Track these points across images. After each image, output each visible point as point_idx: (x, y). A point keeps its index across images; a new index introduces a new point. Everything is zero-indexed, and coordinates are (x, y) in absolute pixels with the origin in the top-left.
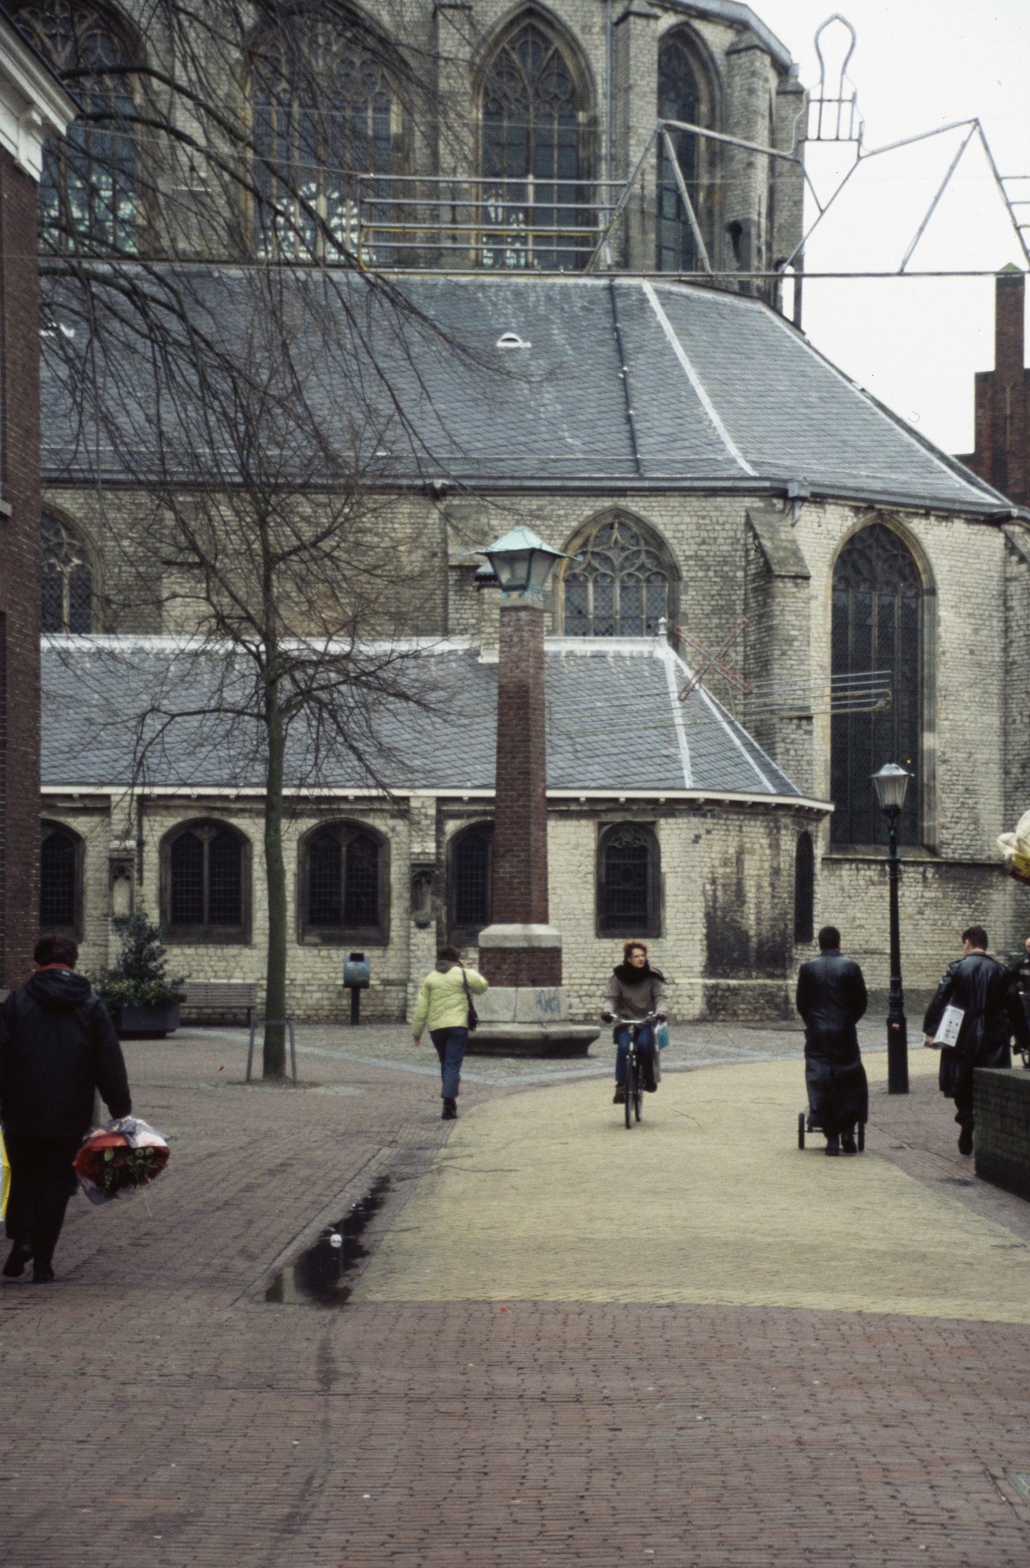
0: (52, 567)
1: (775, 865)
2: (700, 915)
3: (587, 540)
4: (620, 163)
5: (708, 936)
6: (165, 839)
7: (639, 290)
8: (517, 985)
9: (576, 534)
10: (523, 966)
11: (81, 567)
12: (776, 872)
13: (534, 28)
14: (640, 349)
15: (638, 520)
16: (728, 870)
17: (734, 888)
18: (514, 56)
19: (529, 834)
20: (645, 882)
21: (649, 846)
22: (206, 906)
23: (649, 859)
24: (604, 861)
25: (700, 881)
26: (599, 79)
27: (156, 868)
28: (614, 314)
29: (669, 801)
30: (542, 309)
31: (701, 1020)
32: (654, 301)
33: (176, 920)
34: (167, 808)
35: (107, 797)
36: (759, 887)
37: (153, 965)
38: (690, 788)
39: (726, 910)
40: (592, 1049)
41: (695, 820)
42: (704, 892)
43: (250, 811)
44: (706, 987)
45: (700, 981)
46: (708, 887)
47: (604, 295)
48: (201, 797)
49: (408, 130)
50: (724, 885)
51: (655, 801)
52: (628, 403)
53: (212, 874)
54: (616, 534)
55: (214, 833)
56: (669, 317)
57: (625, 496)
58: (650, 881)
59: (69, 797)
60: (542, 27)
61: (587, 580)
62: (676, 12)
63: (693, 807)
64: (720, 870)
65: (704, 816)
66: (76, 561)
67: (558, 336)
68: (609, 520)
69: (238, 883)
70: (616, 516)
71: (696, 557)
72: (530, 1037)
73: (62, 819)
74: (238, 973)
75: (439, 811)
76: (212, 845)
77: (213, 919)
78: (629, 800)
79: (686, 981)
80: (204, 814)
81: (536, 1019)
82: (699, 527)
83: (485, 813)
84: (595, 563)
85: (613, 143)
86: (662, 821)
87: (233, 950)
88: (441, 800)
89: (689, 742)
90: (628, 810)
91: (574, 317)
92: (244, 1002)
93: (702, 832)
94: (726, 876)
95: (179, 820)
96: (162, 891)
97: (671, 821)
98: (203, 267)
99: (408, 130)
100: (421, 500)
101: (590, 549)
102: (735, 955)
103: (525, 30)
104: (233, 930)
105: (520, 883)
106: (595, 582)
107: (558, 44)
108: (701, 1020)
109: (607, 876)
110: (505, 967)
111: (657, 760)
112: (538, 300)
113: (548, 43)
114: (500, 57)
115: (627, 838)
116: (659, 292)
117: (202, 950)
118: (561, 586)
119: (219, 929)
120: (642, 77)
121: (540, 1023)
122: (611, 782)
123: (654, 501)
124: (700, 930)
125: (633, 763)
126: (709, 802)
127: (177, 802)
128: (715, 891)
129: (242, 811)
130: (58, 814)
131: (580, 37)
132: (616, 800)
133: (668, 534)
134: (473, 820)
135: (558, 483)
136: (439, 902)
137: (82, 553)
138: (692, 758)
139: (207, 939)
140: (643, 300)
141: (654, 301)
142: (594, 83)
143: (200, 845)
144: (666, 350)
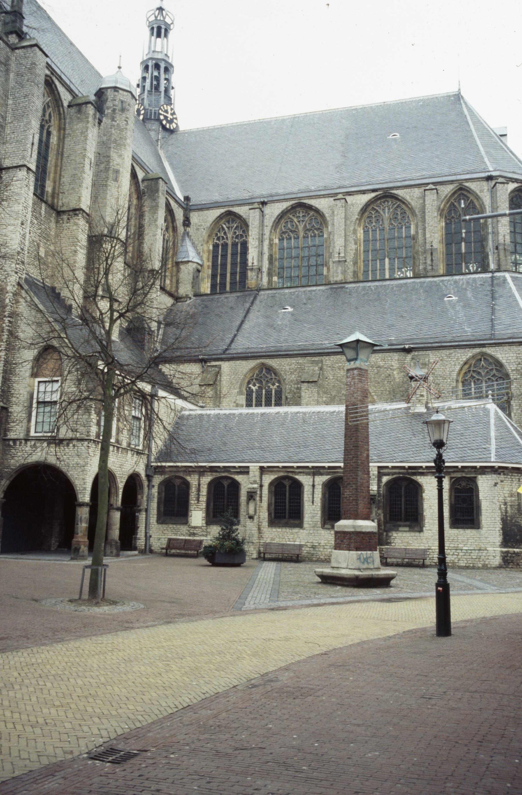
0: (269, 387)
2: (498, 519)
3: (471, 365)
4: (496, 233)
5: (503, 529)
6: (271, 484)
7: (504, 277)
8: (349, 550)
9: (465, 363)
10: (352, 541)
11: (278, 386)
13: (463, 194)
14: (501, 296)
15: (491, 356)
16: (513, 499)
17: (516, 507)
18: (456, 204)
19: (357, 476)
20: (473, 504)
21: (474, 488)
22: (287, 512)
23: (474, 494)
24: (453, 494)
25: (498, 504)
26: (487, 207)
27: (267, 496)
28: (492, 285)
29: (481, 467)
30: (464, 286)
31: (500, 567)
32: (509, 280)
33: (276, 517)
34: (272, 471)
35: (248, 467)
37: (234, 535)
38: (494, 461)
39: (512, 517)
40: (393, 582)
41: (495, 476)
42: (500, 509)
43: (303, 472)
44: (502, 552)
45: (499, 549)
46: (502, 506)
47: (490, 280)
48: (284, 467)
49: (417, 232)
50: (511, 506)
51: (475, 467)
52: (493, 314)
53: (290, 499)
54: (483, 363)
55: (290, 482)
56: (515, 285)
58: (475, 503)
59: (234, 467)
60: (466, 193)
61: (471, 382)
62: (517, 183)
63: (493, 470)
64: (509, 499)
65: (500, 474)
66: (277, 384)
67: (469, 294)
68: (479, 357)
69: (300, 503)
70: (482, 356)
71: (516, 370)
72: (349, 576)
73: (233, 476)
74: (298, 540)
75: (379, 472)
76: (290, 487)
77: (290, 517)
78: (462, 467)
79: (492, 549)
80: (285, 474)
81: (357, 567)
82: (517, 358)
83: (399, 473)
84: (474, 375)
85: (493, 228)
86: (479, 476)
87: (296, 530)
88: (379, 467)
89: (496, 442)
90: (463, 472)
91: (476, 287)
92: (297, 552)
93: (499, 481)
94: (512, 501)
95: (276, 476)
96: (269, 505)
97: (484, 476)
98: (343, 285)
99: (417, 232)
100: (402, 353)
101: (472, 369)
102: (518, 537)
103: (460, 195)
104: (297, 522)
105: (353, 500)
106: (474, 382)
107: (472, 197)
108: (500, 567)
109: (455, 501)
110: (345, 541)
111: (480, 450)
112: (463, 283)
113: (468, 198)
114: (450, 205)
115: (464, 484)
116: (511, 277)
117: (284, 530)
118: (460, 385)
119: (292, 521)
120: (503, 203)
121: (359, 569)
122: (457, 459)
123: (497, 348)
124: (499, 526)
125: (469, 451)
126: (500, 467)
127: (275, 469)
128: (506, 508)
129: (300, 472)
130: (231, 474)
131: (479, 194)
132: (457, 467)
133: (504, 361)
134: (394, 476)
135: (457, 344)
136: (380, 511)
137: (279, 382)
138: (496, 449)
139: (287, 525)
140: (505, 280)
141: (509, 280)
142: (485, 208)
143: (285, 487)
144: (512, 296)
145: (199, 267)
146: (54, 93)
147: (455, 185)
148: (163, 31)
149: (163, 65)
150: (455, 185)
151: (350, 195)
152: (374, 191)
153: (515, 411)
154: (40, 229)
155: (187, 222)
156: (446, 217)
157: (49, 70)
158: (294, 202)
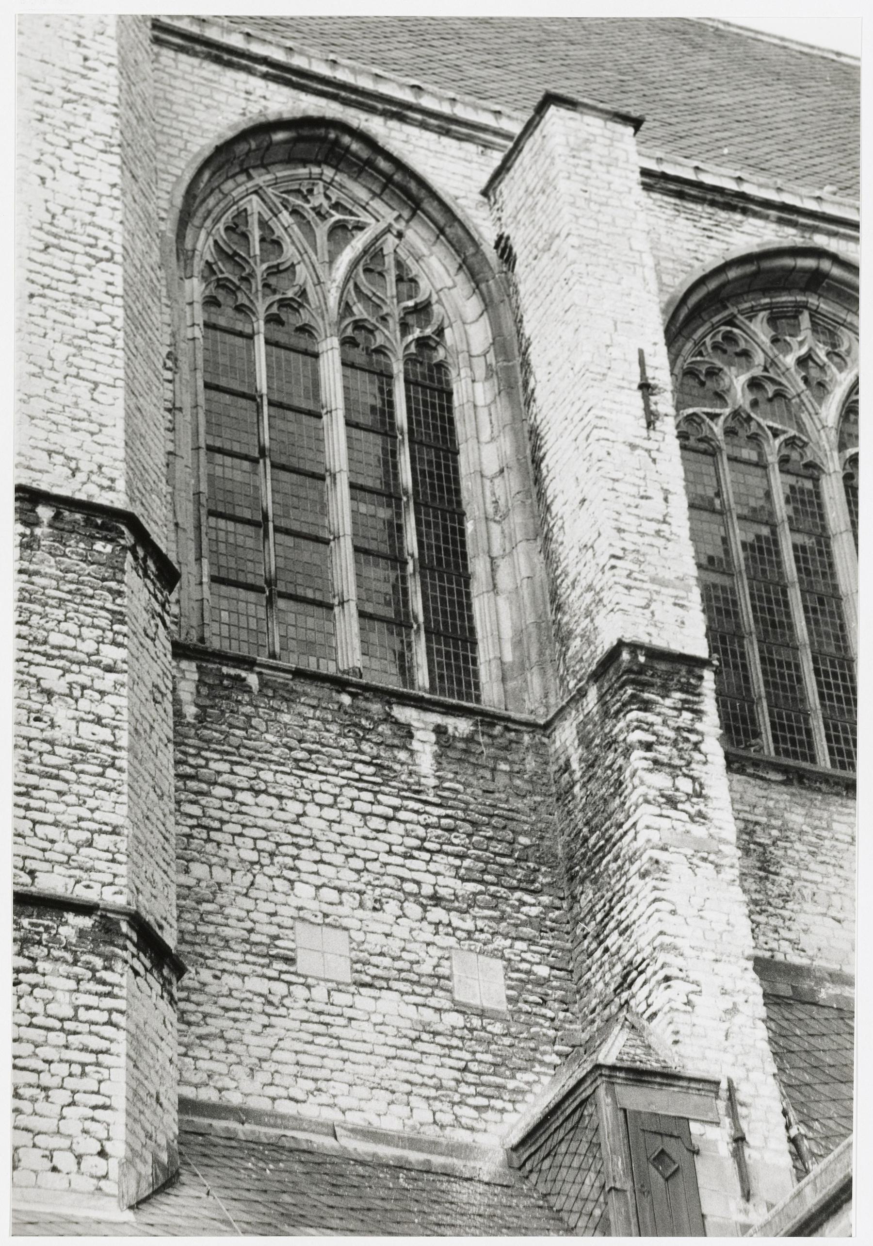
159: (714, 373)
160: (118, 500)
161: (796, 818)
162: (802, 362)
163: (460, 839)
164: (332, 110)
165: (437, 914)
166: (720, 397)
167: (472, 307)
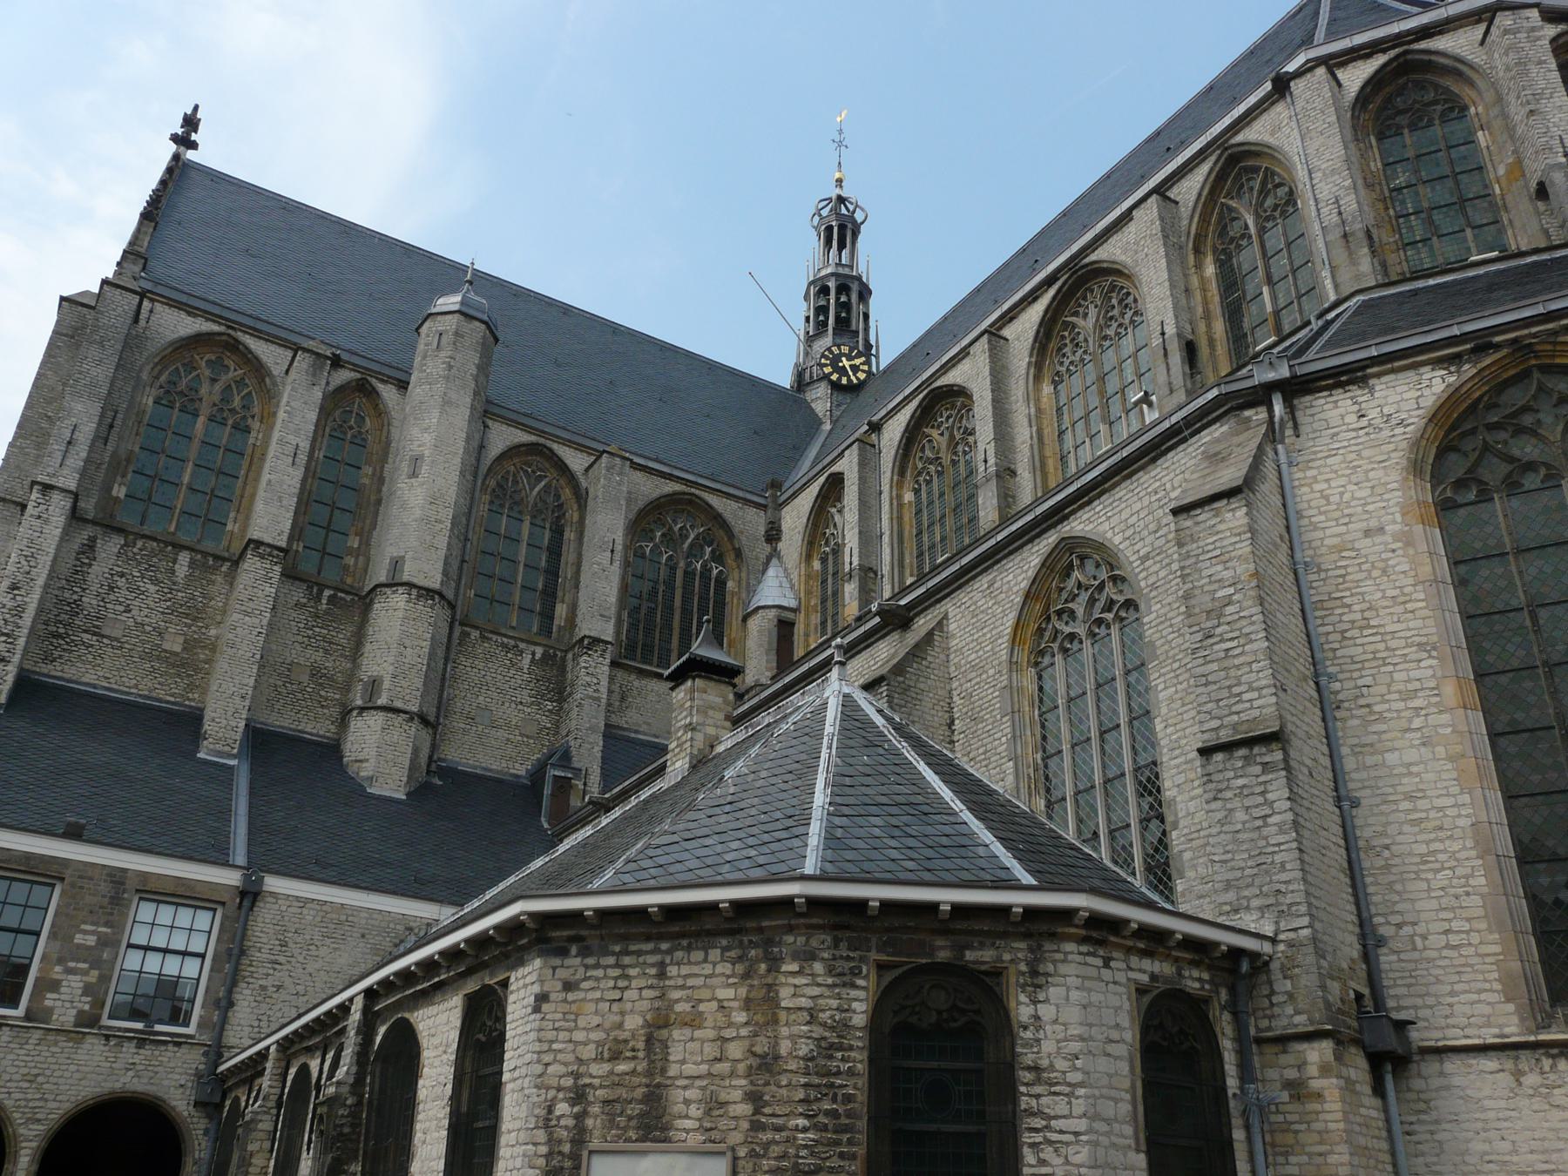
1: (761, 1047)
12: (767, 1064)
36: (713, 1105)
46: (562, 1108)
57: (1066, 518)
65: (563, 952)
103: (1239, 175)
113: (1256, 170)
128: (580, 1117)
145: (790, 615)
146: (249, 360)
147: (1213, 158)
148: (836, 229)
149: (832, 284)
150: (1213, 158)
151: (1012, 319)
152: (1049, 281)
153: (1164, 710)
154: (170, 600)
155: (773, 534)
156: (1215, 249)
157: (220, 324)
158: (921, 396)
159: (652, 531)
160: (437, 586)
161: (636, 683)
162: (681, 529)
163: (532, 685)
164: (542, 441)
165: (520, 707)
166: (652, 539)
167: (575, 507)
